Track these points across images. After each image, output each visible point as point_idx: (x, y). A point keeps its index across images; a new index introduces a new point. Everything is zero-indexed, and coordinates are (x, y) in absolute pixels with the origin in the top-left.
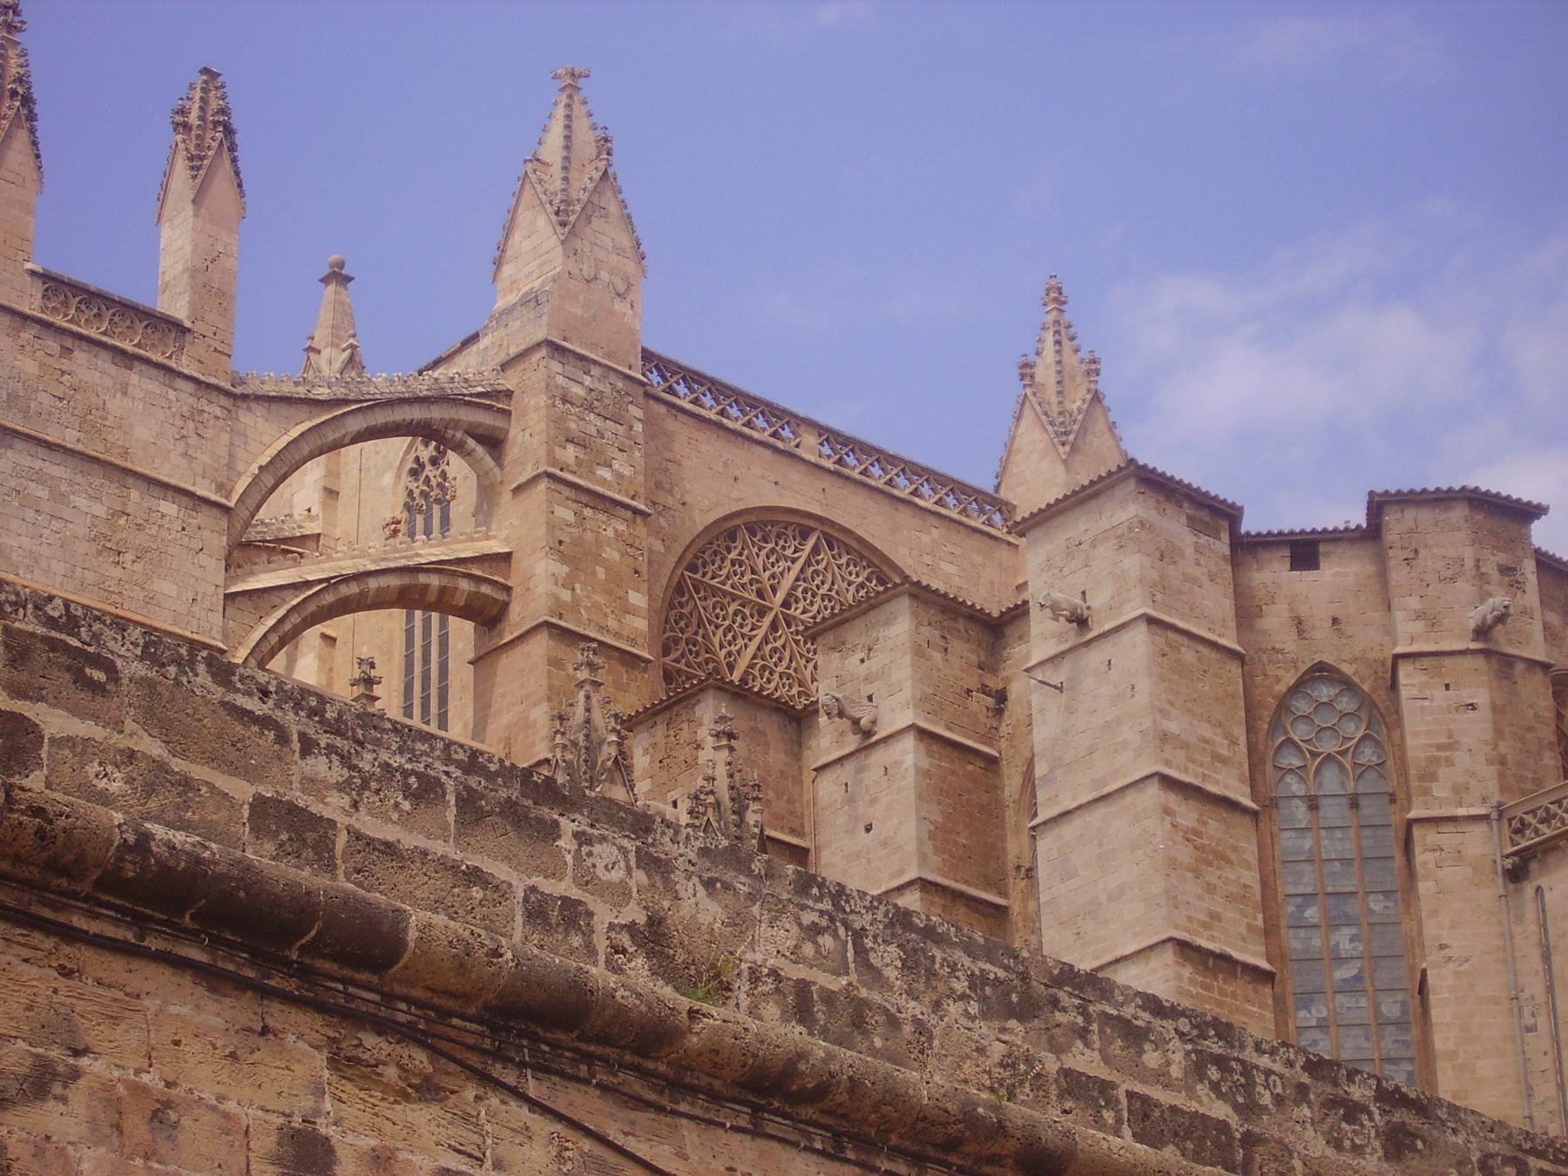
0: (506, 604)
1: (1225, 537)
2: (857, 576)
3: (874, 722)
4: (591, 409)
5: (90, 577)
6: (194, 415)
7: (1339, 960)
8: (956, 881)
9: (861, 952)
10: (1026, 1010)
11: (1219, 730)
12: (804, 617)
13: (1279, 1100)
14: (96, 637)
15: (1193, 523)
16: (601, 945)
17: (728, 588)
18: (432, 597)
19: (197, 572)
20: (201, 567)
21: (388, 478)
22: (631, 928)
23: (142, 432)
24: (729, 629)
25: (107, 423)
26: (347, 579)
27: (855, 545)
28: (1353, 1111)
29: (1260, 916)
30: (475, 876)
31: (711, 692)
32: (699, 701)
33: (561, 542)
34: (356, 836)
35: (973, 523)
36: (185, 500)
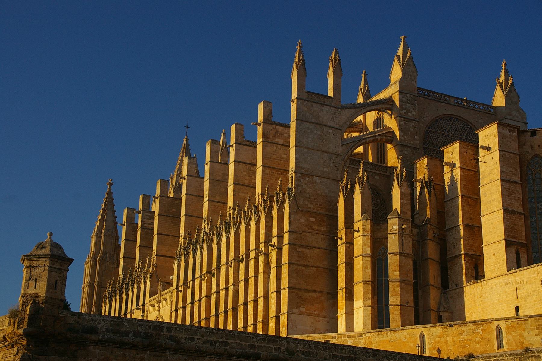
1: (516, 132)
4: (408, 103)
5: (317, 145)
7: (538, 209)
9: (310, 346)
10: (329, 349)
11: (514, 169)
13: (359, 353)
14: (233, 333)
15: (509, 131)
16: (282, 351)
22: (285, 349)
24: (436, 138)
27: (462, 119)
28: (369, 353)
29: (522, 203)
30: (269, 347)
33: (402, 129)
34: (257, 346)
35: (486, 112)
36: (334, 129)
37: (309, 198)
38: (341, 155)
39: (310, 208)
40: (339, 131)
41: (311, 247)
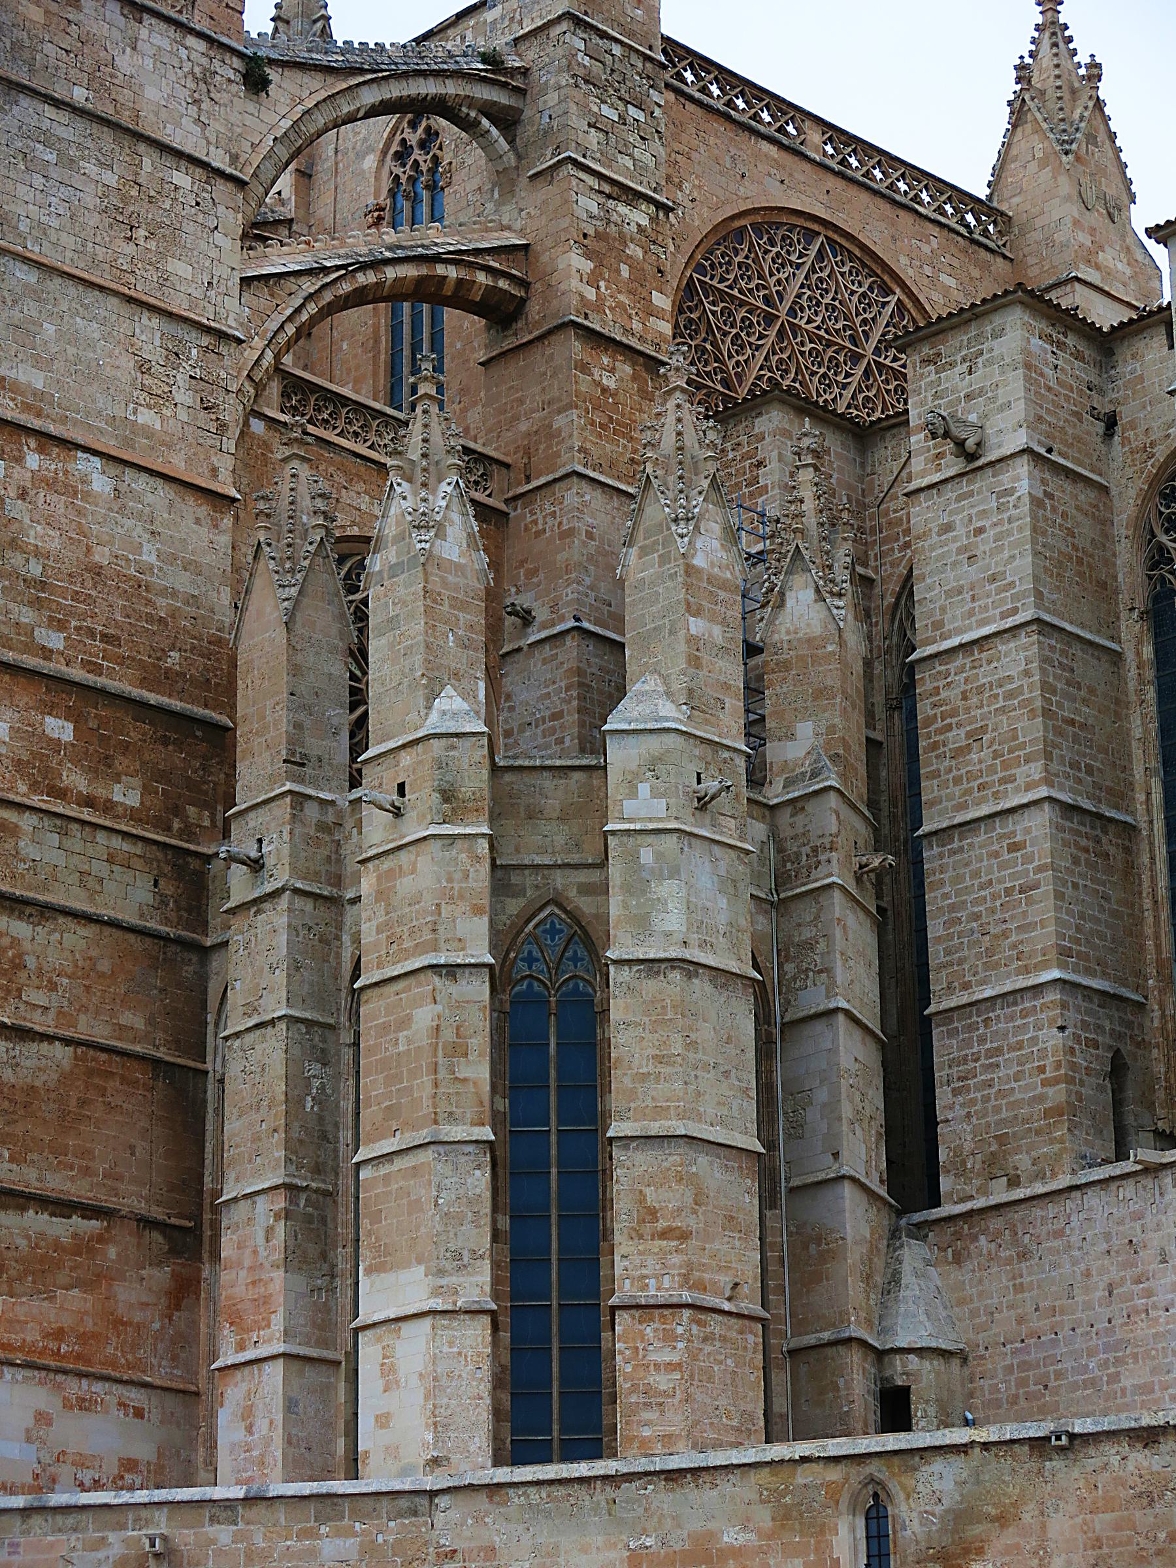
0: (523, 301)
2: (860, 286)
3: (978, 444)
6: (206, 77)
8: (1071, 623)
12: (808, 327)
17: (735, 292)
18: (448, 290)
19: (213, 253)
20: (217, 247)
21: (370, 162)
23: (152, 94)
25: (116, 81)
26: (364, 267)
27: (857, 252)
31: (776, 404)
32: (760, 414)
33: (585, 236)
37: (43, 585)
38: (240, 341)
39: (47, 653)
40: (230, 186)
41: (46, 911)
